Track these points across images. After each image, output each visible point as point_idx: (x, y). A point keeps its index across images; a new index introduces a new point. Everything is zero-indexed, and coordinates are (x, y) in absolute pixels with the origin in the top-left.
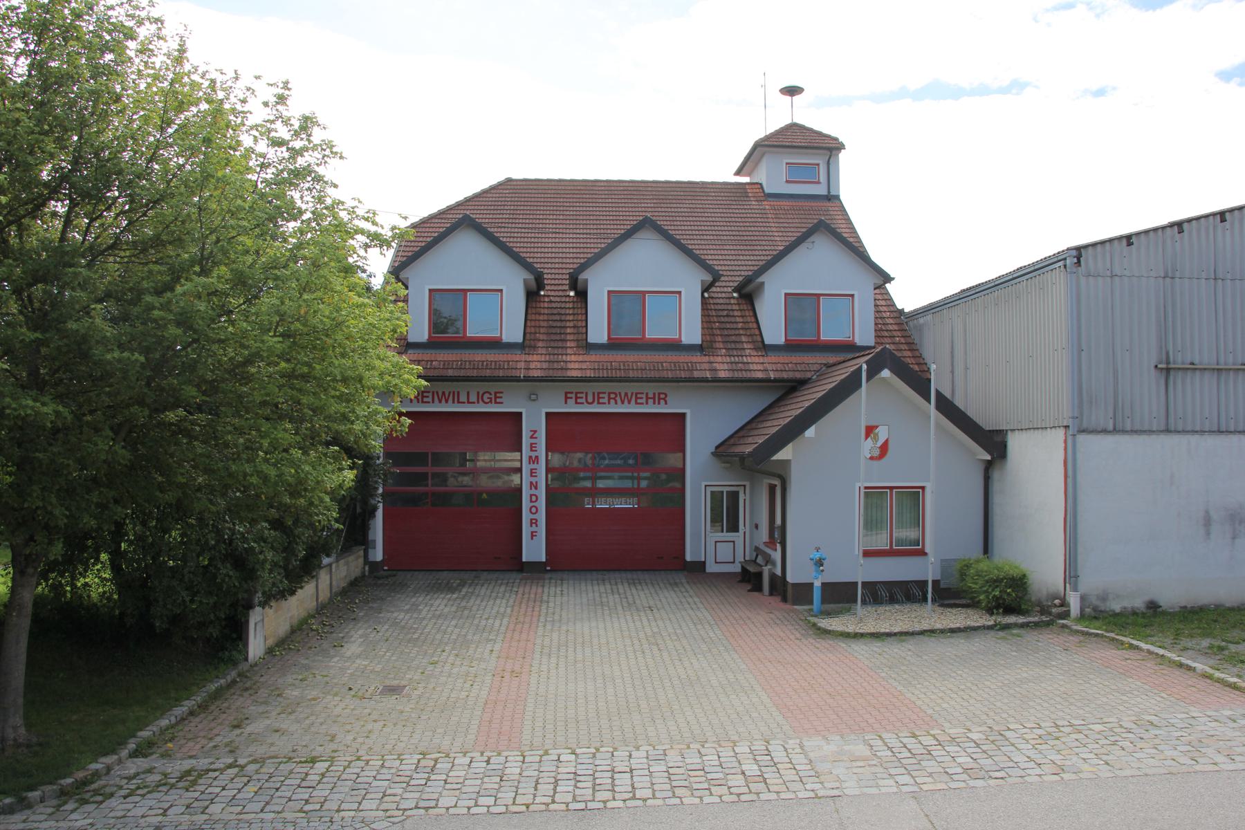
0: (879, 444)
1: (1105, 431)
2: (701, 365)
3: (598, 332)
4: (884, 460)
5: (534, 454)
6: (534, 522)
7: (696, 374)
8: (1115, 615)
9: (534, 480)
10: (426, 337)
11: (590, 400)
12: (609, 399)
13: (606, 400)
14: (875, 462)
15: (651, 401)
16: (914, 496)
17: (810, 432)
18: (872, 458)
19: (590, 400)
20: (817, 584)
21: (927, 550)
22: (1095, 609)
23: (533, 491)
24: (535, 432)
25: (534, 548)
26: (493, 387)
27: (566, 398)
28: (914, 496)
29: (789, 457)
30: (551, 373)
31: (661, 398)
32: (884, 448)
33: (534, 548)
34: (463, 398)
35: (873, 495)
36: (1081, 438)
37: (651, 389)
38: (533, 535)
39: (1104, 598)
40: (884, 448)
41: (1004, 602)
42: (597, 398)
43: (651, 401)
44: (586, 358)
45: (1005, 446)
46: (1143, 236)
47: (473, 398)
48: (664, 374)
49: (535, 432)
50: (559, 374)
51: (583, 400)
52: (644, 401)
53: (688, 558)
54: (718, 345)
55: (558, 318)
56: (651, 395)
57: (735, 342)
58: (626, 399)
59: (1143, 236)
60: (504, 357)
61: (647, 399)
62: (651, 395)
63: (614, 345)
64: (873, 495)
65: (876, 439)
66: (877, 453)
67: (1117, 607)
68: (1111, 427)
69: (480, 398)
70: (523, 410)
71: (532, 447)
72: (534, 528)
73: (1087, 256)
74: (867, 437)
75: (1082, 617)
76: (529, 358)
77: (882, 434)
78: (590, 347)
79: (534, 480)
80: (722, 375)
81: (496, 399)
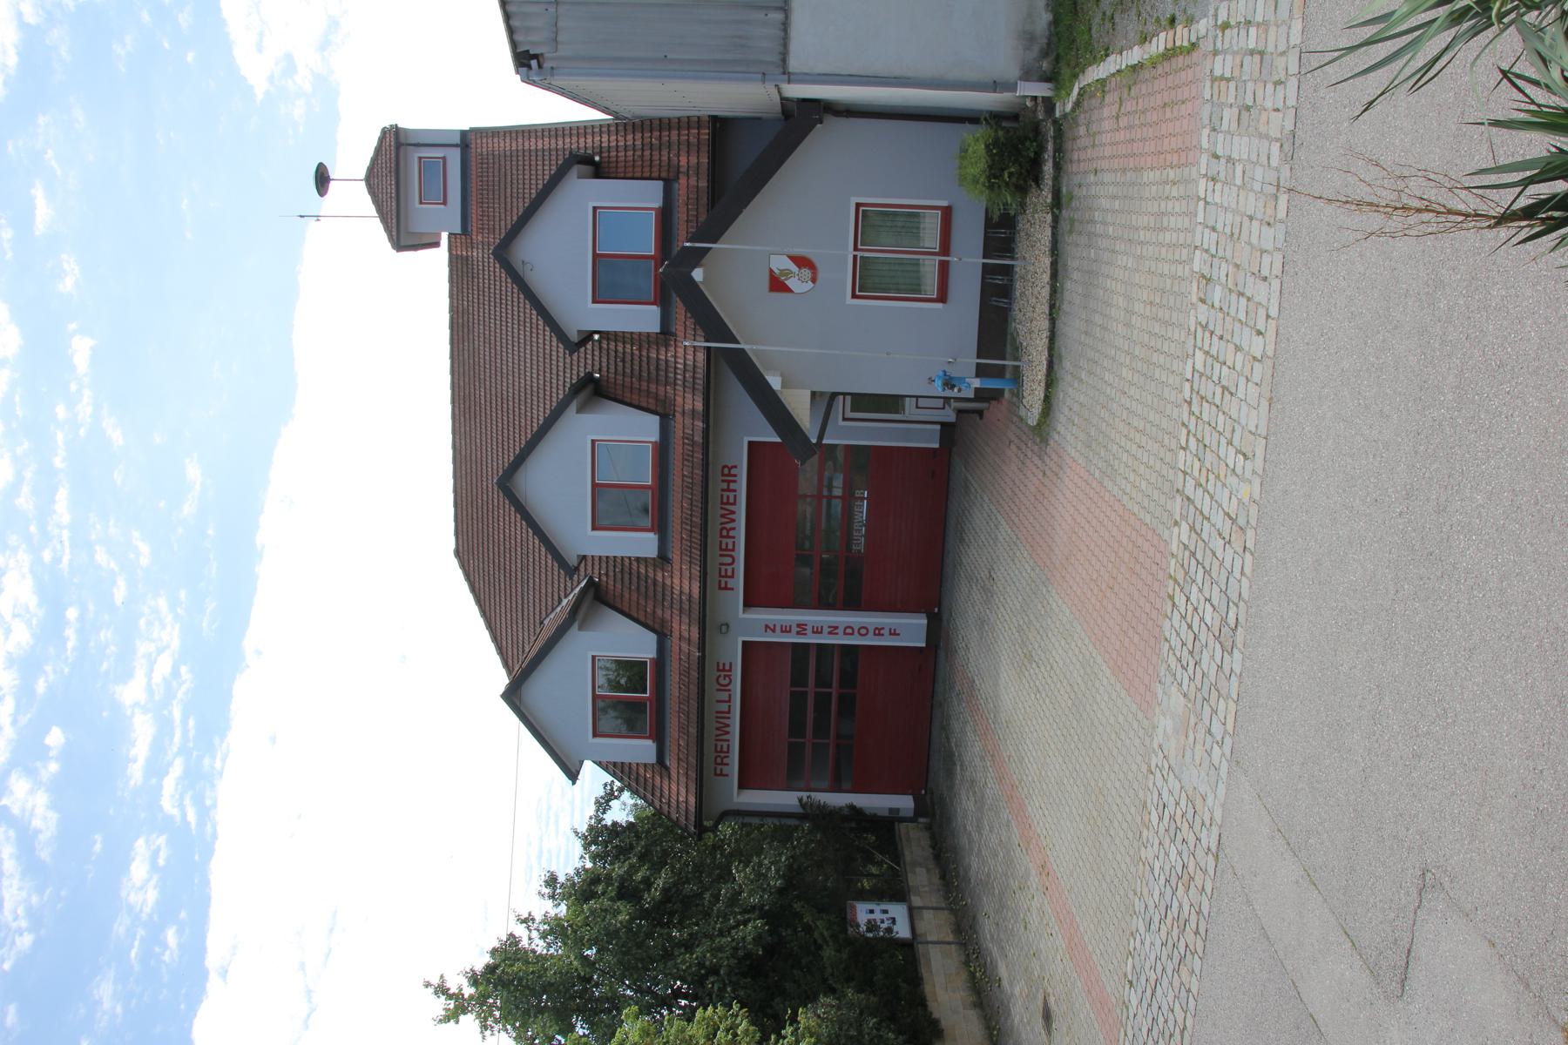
0: (794, 268)
1: (785, 26)
2: (687, 427)
3: (644, 544)
4: (818, 265)
5: (795, 629)
6: (878, 632)
7: (698, 438)
8: (1056, 22)
9: (826, 630)
10: (649, 743)
11: (729, 560)
12: (728, 537)
13: (730, 541)
14: (821, 275)
15: (732, 486)
16: (868, 221)
17: (775, 382)
18: (814, 280)
19: (729, 560)
20: (977, 383)
21: (945, 203)
22: (1045, 54)
23: (840, 631)
24: (767, 627)
25: (909, 630)
26: (711, 674)
27: (726, 588)
28: (868, 221)
29: (808, 393)
30: (695, 615)
31: (728, 474)
32: (801, 262)
33: (909, 630)
34: (724, 707)
35: (868, 281)
36: (794, 64)
37: (716, 485)
38: (893, 633)
39: (1029, 38)
40: (801, 262)
41: (1022, 154)
42: (728, 551)
43: (732, 486)
44: (676, 567)
45: (805, 100)
46: (512, 22)
47: (724, 696)
48: (698, 479)
49: (767, 627)
50: (696, 607)
51: (729, 568)
52: (731, 495)
53: (937, 446)
54: (662, 393)
55: (627, 576)
56: (725, 486)
57: (657, 369)
58: (729, 516)
59: (512, 22)
60: (675, 665)
61: (729, 490)
62: (725, 486)
63: (661, 527)
64: (868, 281)
65: (788, 273)
66: (807, 273)
67: (1045, 17)
68: (779, 16)
69: (725, 688)
70: (740, 640)
71: (786, 630)
72: (886, 632)
73: (534, 42)
74: (787, 289)
75: (1051, 78)
76: (676, 634)
77: (781, 263)
78: (663, 558)
79: (826, 630)
80: (699, 406)
81: (726, 670)
